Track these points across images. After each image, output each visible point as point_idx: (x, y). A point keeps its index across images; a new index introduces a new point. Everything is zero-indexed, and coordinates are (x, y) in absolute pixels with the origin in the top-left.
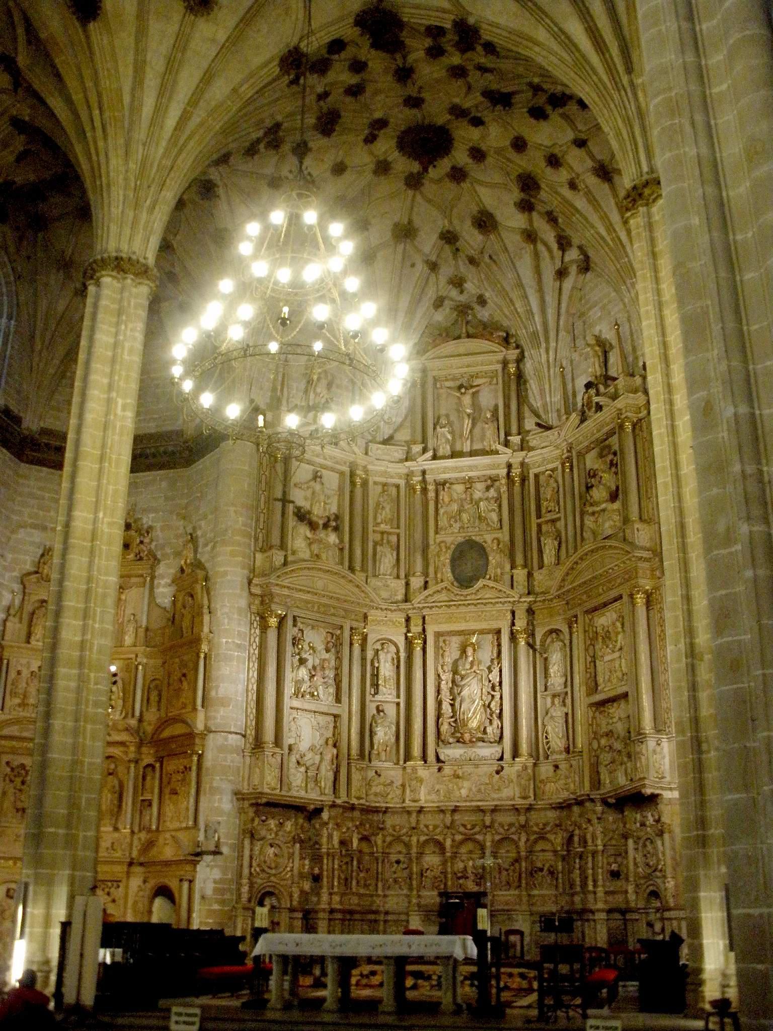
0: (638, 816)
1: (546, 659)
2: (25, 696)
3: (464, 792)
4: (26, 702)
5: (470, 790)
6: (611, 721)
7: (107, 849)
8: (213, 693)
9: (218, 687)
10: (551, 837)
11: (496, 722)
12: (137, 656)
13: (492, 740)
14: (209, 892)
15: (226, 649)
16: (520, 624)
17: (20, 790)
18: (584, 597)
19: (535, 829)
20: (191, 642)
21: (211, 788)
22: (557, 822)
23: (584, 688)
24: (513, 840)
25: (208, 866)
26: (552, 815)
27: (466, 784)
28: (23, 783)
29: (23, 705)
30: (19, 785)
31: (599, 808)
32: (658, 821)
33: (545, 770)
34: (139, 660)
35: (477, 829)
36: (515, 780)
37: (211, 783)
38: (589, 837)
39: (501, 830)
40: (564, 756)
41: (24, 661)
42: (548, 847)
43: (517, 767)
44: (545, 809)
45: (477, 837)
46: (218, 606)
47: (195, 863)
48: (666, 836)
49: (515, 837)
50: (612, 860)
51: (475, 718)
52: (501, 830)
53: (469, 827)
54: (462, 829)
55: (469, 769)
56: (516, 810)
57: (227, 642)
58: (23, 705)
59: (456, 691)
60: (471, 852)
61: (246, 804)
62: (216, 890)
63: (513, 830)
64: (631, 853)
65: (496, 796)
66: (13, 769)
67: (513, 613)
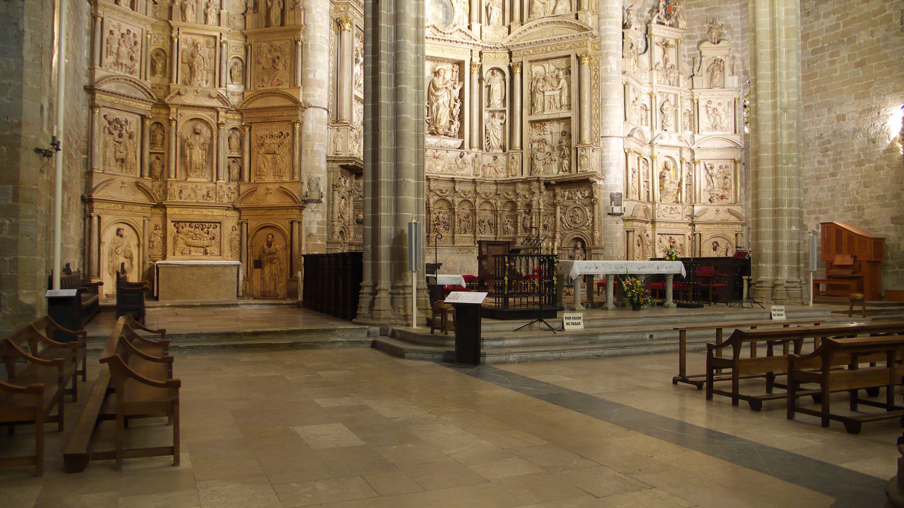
0: (567, 193)
1: (489, 87)
2: (118, 54)
3: (439, 168)
4: (120, 61)
5: (444, 166)
6: (542, 133)
7: (204, 196)
8: (311, 76)
9: (315, 72)
10: (493, 201)
11: (457, 123)
12: (221, 34)
13: (452, 135)
14: (314, 231)
15: (321, 42)
16: (476, 60)
17: (117, 142)
18: (531, 51)
19: (483, 196)
20: (292, 30)
21: (312, 151)
22: (499, 192)
23: (526, 111)
24: (468, 201)
25: (313, 211)
26: (494, 187)
27: (441, 162)
28: (120, 136)
29: (117, 63)
30: (117, 139)
31: (543, 187)
32: (591, 196)
33: (487, 159)
34: (224, 39)
35: (448, 193)
36: (471, 163)
37: (313, 147)
38: (534, 203)
39: (462, 195)
40: (501, 151)
41: (115, 23)
42: (488, 207)
43: (473, 155)
44: (490, 183)
45: (448, 198)
46: (312, 6)
47: (301, 208)
48: (596, 207)
49: (471, 200)
50: (544, 218)
51: (444, 119)
52: (462, 195)
53: (444, 191)
54: (438, 192)
55: (441, 153)
56: (474, 182)
57: (321, 36)
58: (117, 63)
59: (433, 98)
60: (441, 208)
61: (336, 165)
62: (319, 230)
63: (470, 195)
64: (558, 215)
65: (458, 172)
66: (109, 122)
67: (471, 51)
